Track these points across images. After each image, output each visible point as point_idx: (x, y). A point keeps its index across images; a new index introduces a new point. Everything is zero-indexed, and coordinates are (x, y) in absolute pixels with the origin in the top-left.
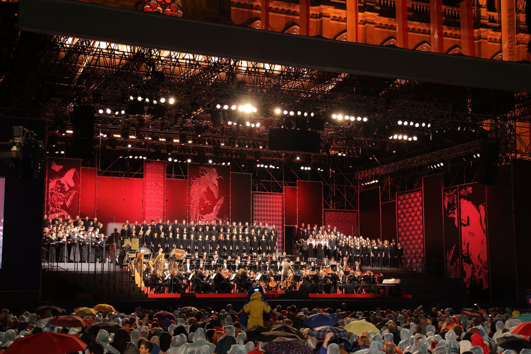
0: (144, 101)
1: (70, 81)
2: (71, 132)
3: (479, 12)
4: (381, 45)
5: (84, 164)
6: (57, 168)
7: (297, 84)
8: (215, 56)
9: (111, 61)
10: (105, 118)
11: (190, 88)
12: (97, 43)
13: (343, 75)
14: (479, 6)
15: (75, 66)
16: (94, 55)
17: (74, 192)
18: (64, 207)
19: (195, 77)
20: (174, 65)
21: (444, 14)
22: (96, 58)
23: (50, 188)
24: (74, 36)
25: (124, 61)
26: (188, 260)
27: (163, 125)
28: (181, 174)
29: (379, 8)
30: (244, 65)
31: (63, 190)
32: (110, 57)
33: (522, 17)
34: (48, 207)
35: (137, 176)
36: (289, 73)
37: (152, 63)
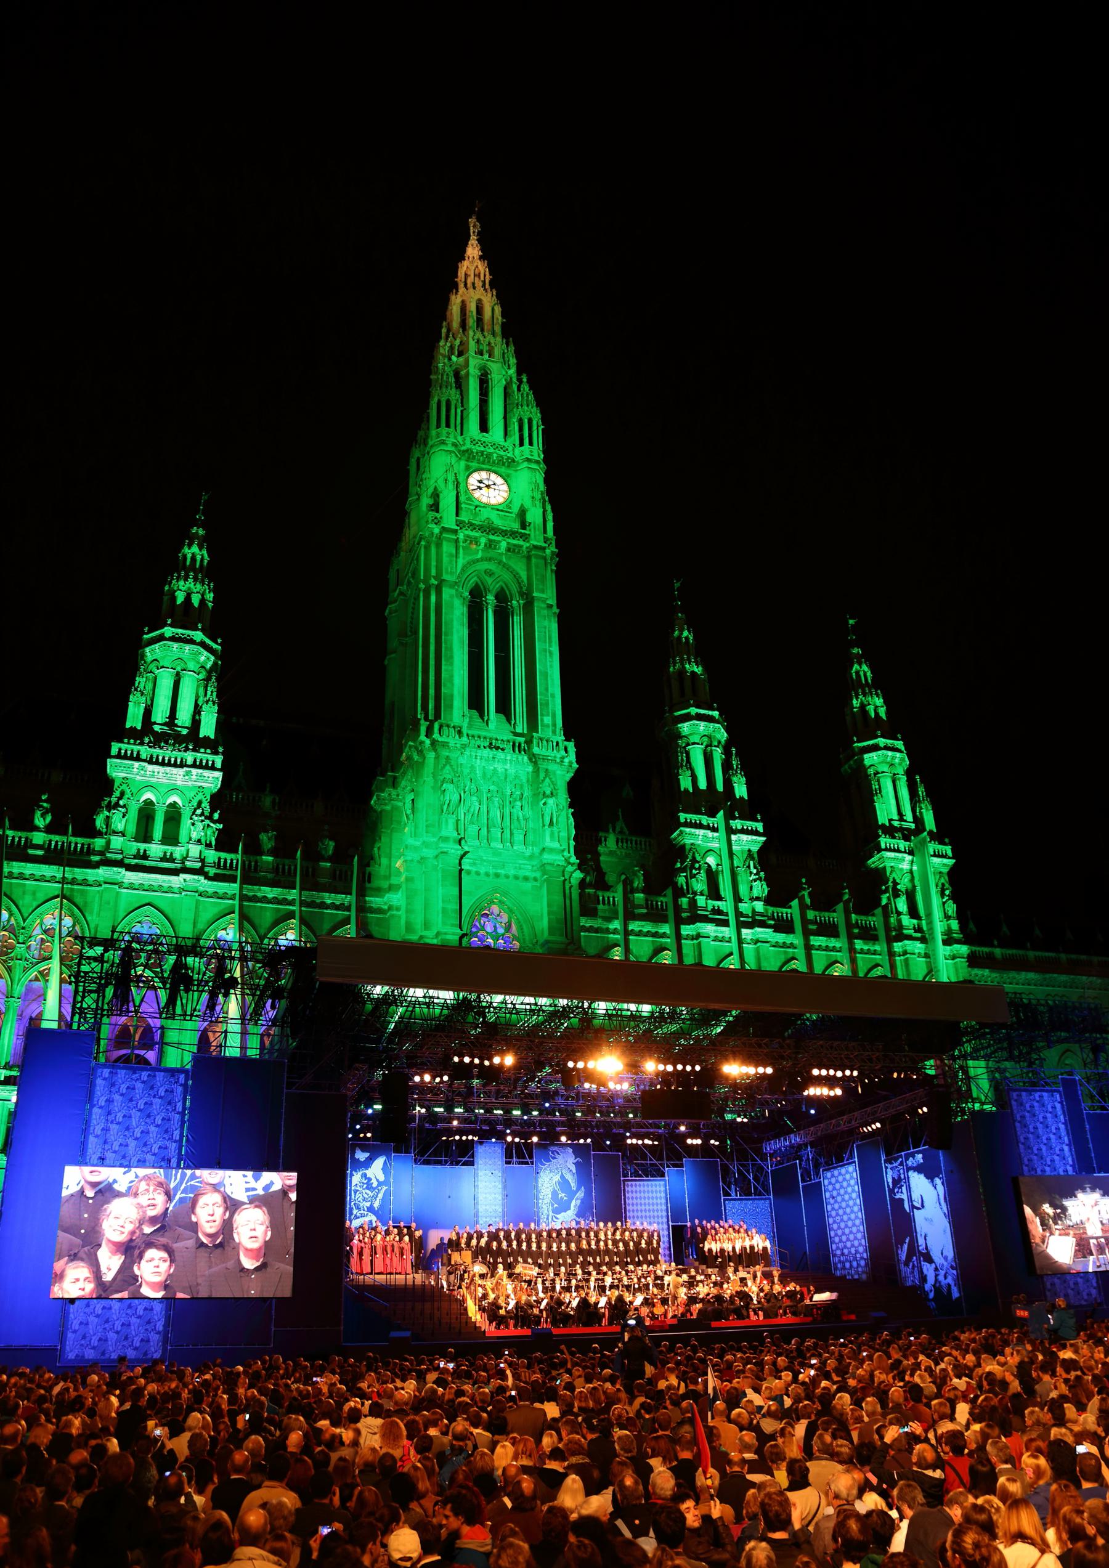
1: (378, 1041)
2: (378, 1107)
3: (899, 921)
4: (780, 970)
5: (397, 1150)
6: (361, 1156)
7: (674, 1028)
8: (563, 998)
10: (422, 1088)
12: (412, 990)
13: (734, 1013)
14: (899, 913)
15: (384, 1021)
17: (384, 1188)
18: (371, 1209)
19: (537, 1026)
21: (857, 925)
22: (410, 1009)
23: (353, 1184)
24: (383, 984)
25: (445, 1012)
26: (540, 1280)
27: (498, 1092)
28: (524, 1157)
29: (772, 922)
31: (369, 1187)
32: (428, 1007)
33: (955, 925)
34: (351, 1209)
35: (466, 1164)
36: (662, 1013)
37: (482, 1012)
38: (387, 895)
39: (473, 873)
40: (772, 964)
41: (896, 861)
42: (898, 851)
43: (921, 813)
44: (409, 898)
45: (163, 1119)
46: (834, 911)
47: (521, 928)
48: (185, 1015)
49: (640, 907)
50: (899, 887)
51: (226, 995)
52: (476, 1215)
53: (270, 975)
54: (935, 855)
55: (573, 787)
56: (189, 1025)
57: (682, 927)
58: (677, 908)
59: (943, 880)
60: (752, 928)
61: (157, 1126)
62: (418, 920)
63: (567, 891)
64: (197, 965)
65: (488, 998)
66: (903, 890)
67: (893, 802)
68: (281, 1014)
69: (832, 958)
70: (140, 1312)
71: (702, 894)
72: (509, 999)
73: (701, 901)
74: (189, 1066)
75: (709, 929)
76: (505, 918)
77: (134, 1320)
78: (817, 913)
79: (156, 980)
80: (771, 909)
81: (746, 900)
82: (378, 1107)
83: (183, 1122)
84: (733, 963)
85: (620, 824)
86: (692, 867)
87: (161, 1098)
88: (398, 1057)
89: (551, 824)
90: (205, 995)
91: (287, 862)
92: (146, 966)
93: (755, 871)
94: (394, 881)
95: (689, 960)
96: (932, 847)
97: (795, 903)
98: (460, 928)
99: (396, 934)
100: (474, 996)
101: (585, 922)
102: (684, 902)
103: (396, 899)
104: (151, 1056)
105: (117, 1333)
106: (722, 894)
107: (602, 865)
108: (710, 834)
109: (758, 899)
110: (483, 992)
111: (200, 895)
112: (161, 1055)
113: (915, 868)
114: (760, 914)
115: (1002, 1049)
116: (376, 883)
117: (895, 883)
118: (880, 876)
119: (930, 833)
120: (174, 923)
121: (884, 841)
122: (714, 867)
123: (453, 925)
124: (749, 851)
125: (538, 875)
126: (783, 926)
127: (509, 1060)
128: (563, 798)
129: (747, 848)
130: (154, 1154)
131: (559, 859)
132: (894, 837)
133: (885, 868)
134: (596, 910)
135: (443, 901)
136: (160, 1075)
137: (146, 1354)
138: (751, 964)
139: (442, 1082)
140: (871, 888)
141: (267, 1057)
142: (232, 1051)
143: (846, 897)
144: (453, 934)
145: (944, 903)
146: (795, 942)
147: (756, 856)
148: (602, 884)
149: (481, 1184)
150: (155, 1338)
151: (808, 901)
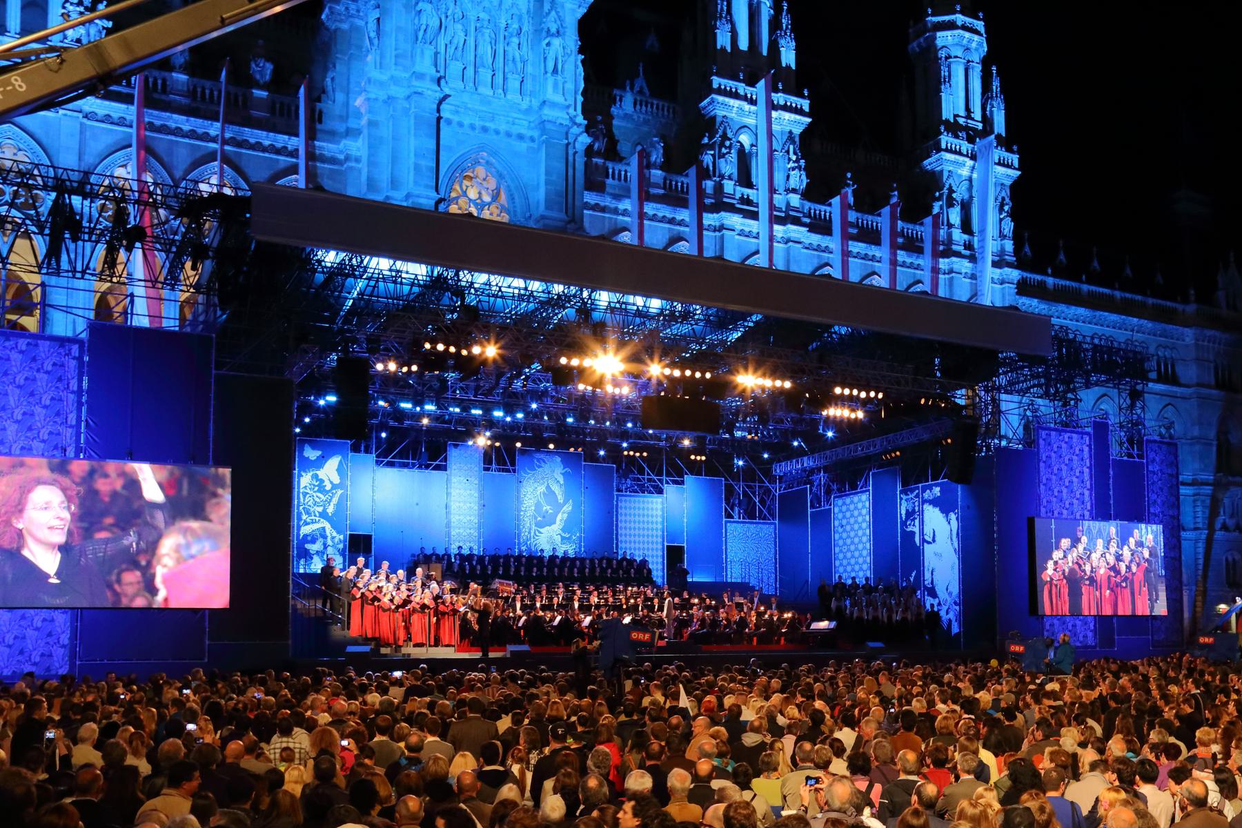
0: (447, 350)
1: (332, 320)
2: (332, 399)
3: (950, 235)
4: (813, 274)
5: (356, 449)
6: (311, 454)
7: (685, 329)
8: (559, 283)
9: (395, 288)
10: (387, 378)
11: (519, 331)
12: (375, 260)
13: (754, 318)
14: (950, 226)
15: (339, 297)
16: (369, 279)
17: (340, 492)
18: (323, 515)
19: (526, 318)
20: (496, 296)
21: (902, 234)
22: (372, 283)
23: (303, 484)
24: (338, 249)
25: (416, 289)
26: (518, 597)
27: (477, 388)
28: (505, 464)
29: (807, 220)
30: (604, 298)
31: (321, 489)
32: (395, 282)
33: (1009, 246)
34: (299, 514)
35: (437, 468)
36: (672, 313)
37: (460, 292)
38: (344, 142)
39: (454, 124)
40: (804, 265)
41: (955, 165)
42: (960, 153)
43: (991, 112)
44: (372, 148)
45: (52, 399)
46: (879, 215)
47: (511, 198)
48: (74, 271)
49: (657, 186)
50: (954, 195)
51: (129, 249)
52: (448, 525)
53: (188, 229)
54: (999, 164)
55: (586, 26)
56: (81, 284)
57: (705, 215)
58: (701, 193)
59: (1003, 194)
60: (784, 224)
61: (45, 407)
62: (384, 177)
63: (571, 158)
64: (86, 210)
65: (469, 277)
66: (959, 199)
67: (962, 94)
68: (206, 276)
69: (873, 266)
70: (38, 622)
71: (730, 178)
72: (496, 279)
73: (729, 186)
74: (83, 335)
75: (734, 220)
76: (492, 184)
77: (30, 633)
78: (859, 215)
79: (28, 222)
80: (807, 205)
81: (781, 190)
82: (332, 399)
83: (80, 404)
84: (761, 261)
85: (640, 82)
86: (722, 145)
87: (48, 372)
88: (355, 341)
89: (555, 71)
90: (101, 250)
91: (208, 84)
92: (12, 205)
93: (794, 158)
94: (352, 124)
95: (709, 252)
96: (999, 153)
97: (836, 201)
98: (437, 191)
99: (356, 188)
100: (451, 274)
101: (590, 198)
102: (709, 185)
103: (356, 147)
104: (30, 323)
105: (9, 646)
106: (754, 180)
107: (615, 131)
108: (746, 107)
109: (794, 191)
110: (463, 269)
111: (86, 117)
112: (43, 322)
113: (975, 176)
114: (796, 209)
115: (1039, 385)
116: (328, 124)
117: (951, 191)
118: (934, 181)
119: (998, 137)
120: (51, 152)
121: (946, 140)
122: (747, 147)
123: (426, 186)
124: (790, 132)
125: (536, 134)
126: (821, 226)
127: (491, 351)
128: (572, 39)
129: (788, 129)
130: (43, 441)
131: (562, 117)
132: (957, 137)
133: (942, 171)
134: (604, 183)
135: (416, 155)
136: (44, 345)
137: (48, 669)
138: (780, 264)
139: (410, 371)
140: (922, 194)
141: (188, 329)
142: (141, 320)
143: (894, 200)
144: (428, 198)
145: (1001, 220)
146: (831, 246)
147: (797, 139)
148: (612, 153)
149: (454, 492)
150: (60, 653)
151: (851, 200)
